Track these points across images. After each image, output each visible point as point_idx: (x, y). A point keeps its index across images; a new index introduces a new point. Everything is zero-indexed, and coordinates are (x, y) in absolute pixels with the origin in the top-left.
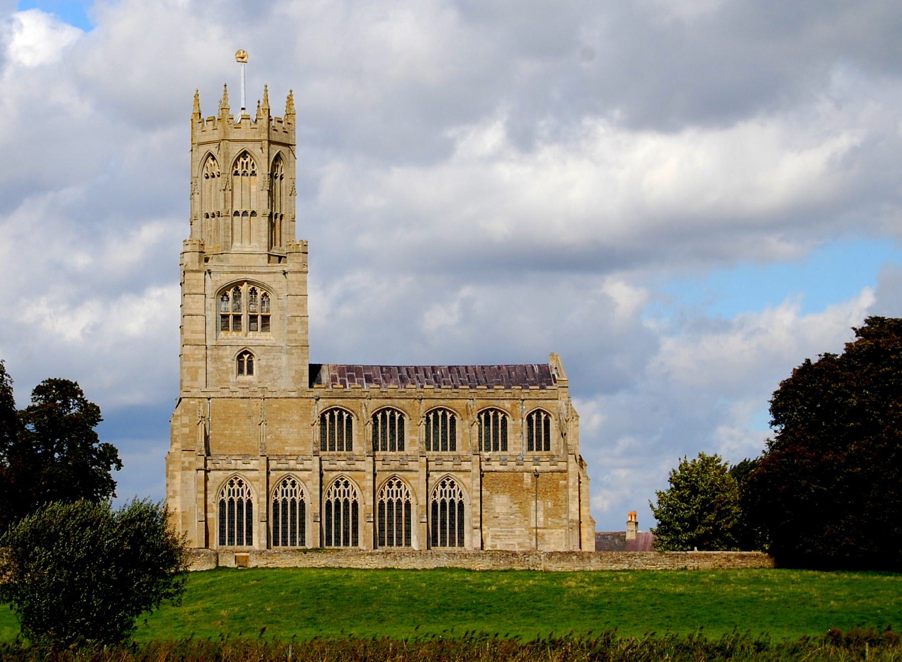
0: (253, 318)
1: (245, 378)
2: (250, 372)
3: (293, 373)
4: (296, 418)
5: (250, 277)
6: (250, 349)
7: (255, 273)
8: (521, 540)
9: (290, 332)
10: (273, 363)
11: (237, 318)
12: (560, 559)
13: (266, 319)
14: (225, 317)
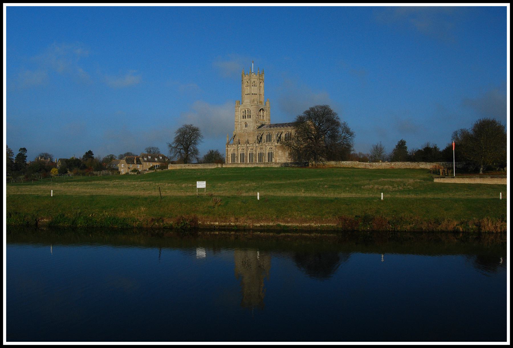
0: (248, 116)
1: (246, 128)
2: (247, 127)
3: (253, 126)
4: (252, 136)
5: (247, 107)
6: (246, 122)
7: (246, 106)
8: (284, 160)
9: (253, 118)
10: (250, 125)
11: (245, 116)
12: (277, 164)
13: (250, 116)
14: (243, 116)
